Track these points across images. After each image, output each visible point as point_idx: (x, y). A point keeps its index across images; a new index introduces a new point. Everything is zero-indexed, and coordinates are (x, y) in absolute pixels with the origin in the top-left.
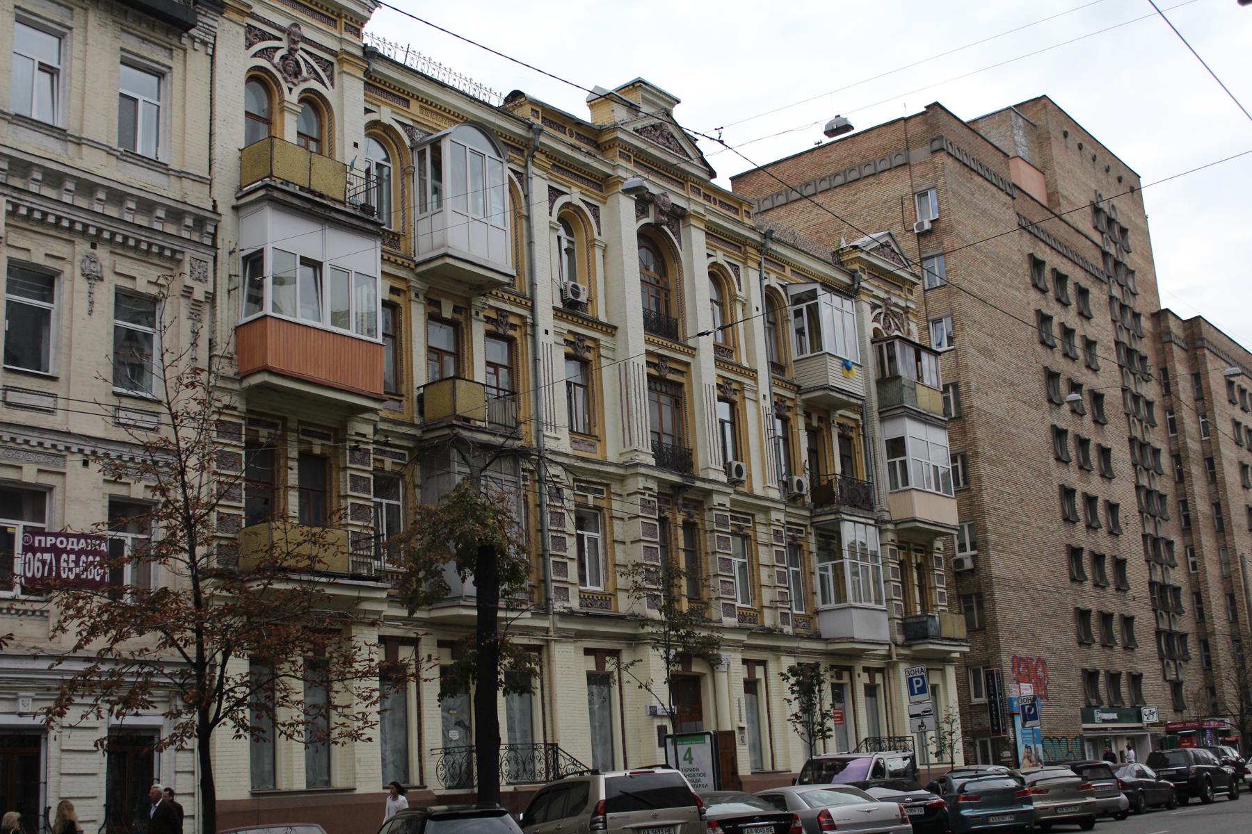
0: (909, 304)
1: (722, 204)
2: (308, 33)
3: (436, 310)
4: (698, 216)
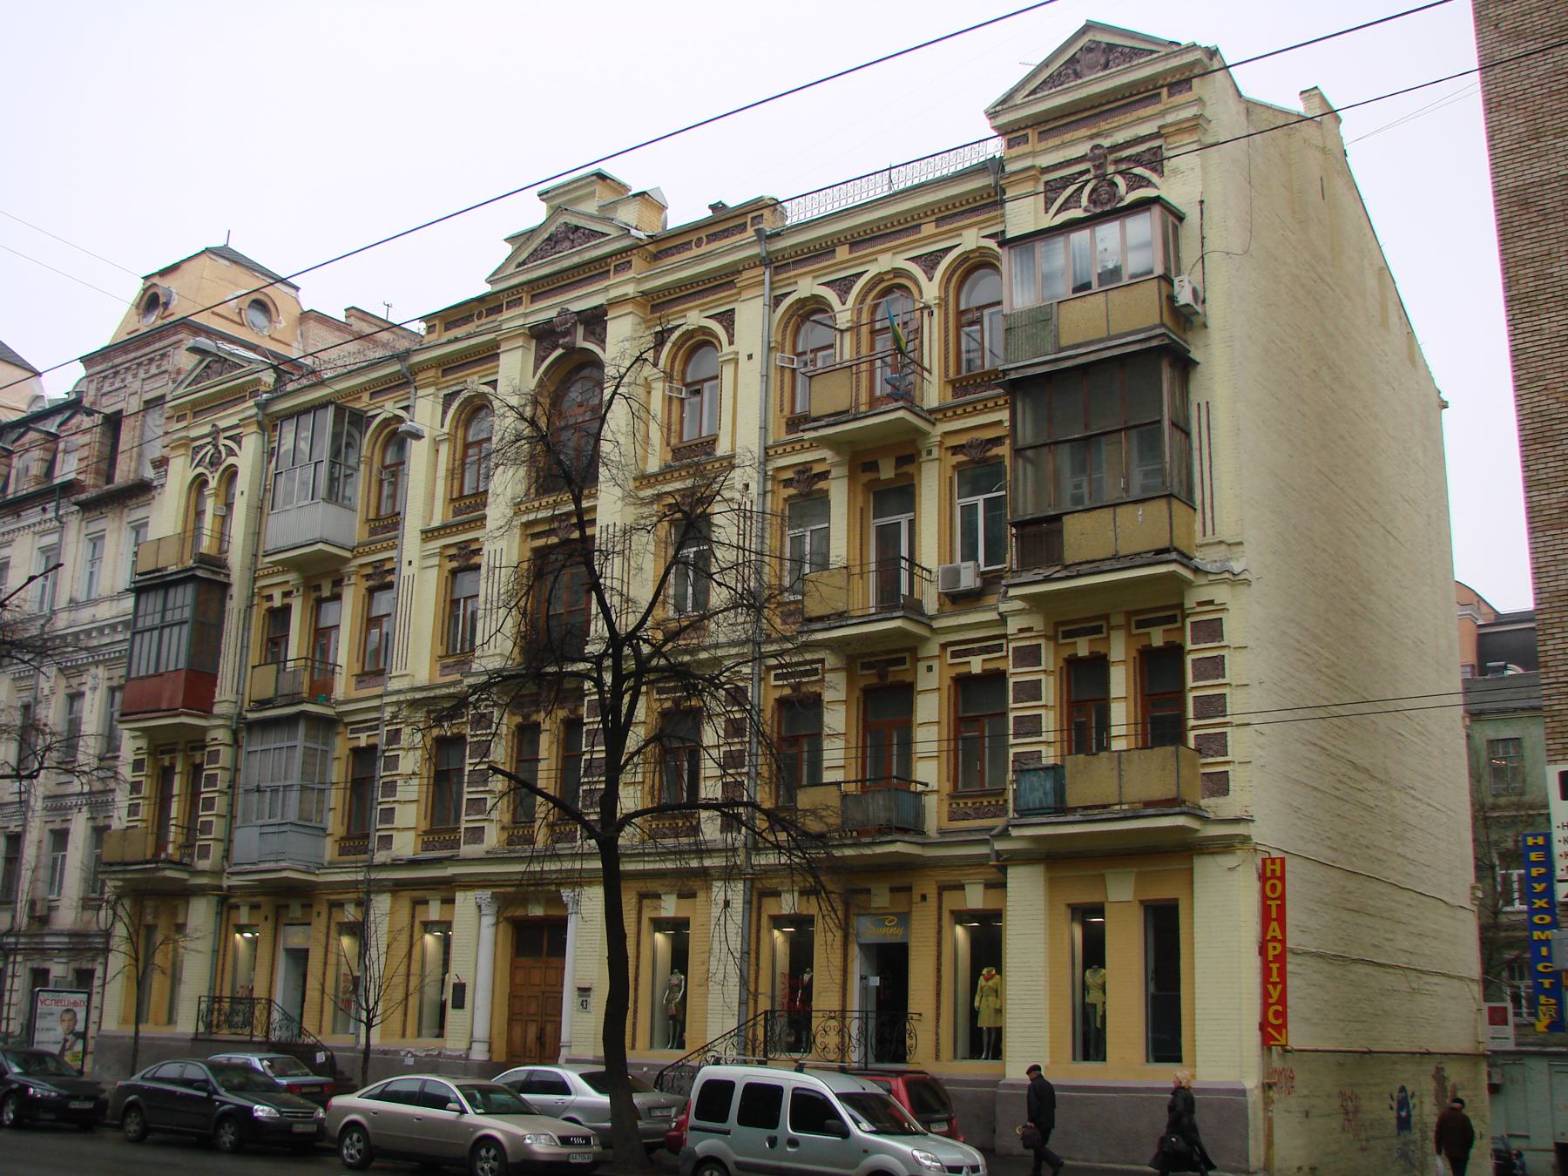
0: (1170, 118)
1: (713, 238)
2: (222, 424)
3: (317, 594)
4: (614, 303)
